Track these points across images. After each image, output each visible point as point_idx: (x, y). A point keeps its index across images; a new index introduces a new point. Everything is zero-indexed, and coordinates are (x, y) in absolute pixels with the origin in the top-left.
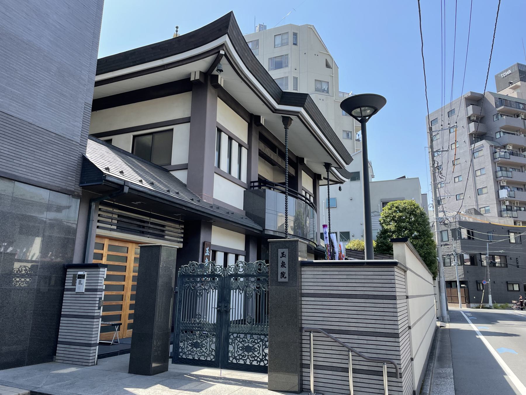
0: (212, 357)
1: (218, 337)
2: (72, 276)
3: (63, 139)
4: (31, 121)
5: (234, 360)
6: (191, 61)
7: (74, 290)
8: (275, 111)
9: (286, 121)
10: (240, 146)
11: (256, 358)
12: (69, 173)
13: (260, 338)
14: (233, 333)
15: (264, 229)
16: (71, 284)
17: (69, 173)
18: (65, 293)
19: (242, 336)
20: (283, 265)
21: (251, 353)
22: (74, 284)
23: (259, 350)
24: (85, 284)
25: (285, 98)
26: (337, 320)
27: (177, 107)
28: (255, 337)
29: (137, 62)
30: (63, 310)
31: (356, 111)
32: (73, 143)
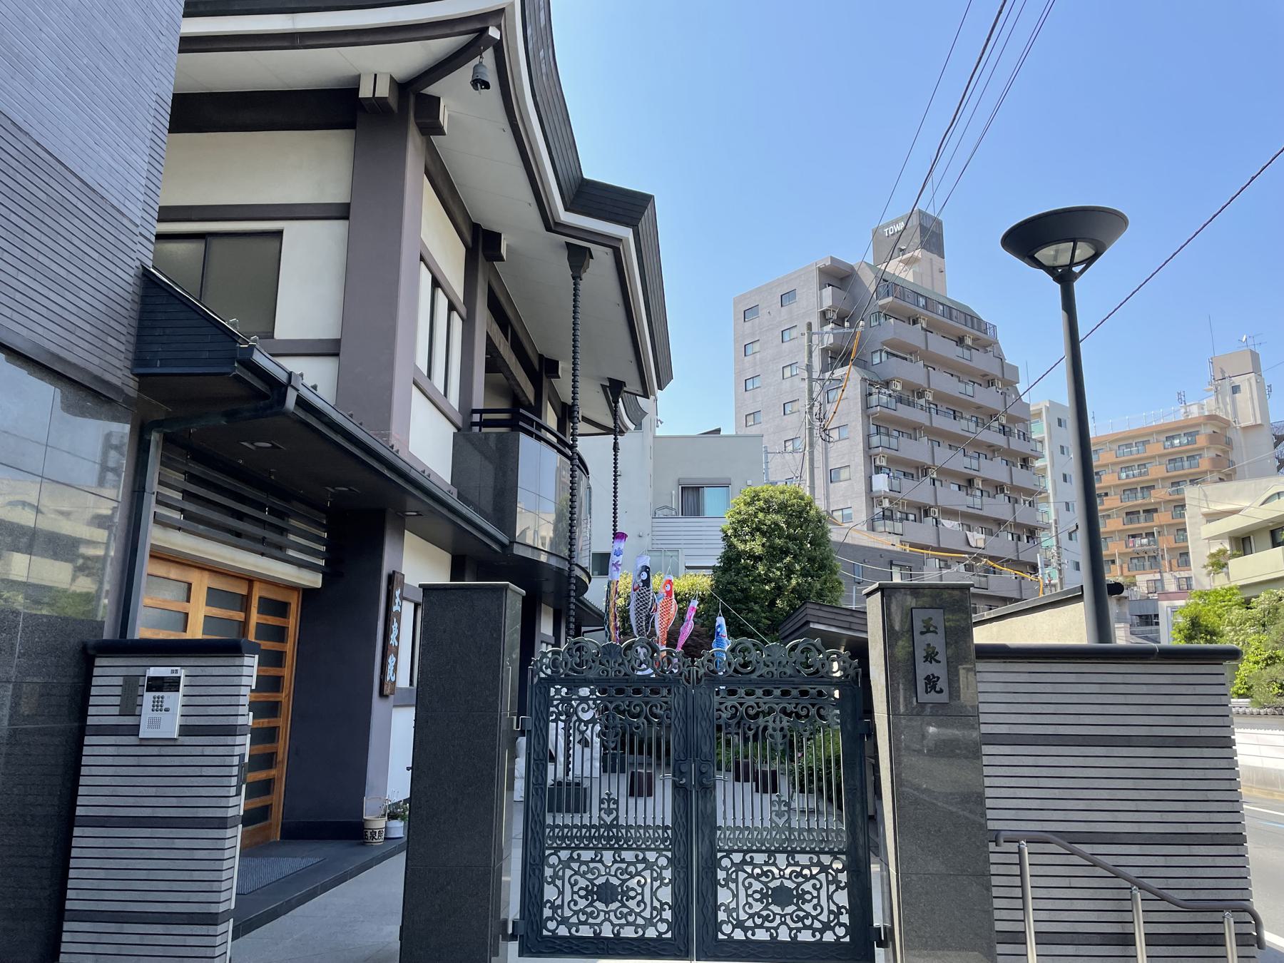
0: (663, 927)
1: (680, 864)
2: (120, 681)
3: (98, 200)
4: (19, 120)
5: (738, 931)
6: (387, 38)
7: (135, 730)
8: (551, 225)
9: (578, 258)
10: (452, 307)
11: (808, 922)
12: (113, 323)
13: (819, 864)
14: (729, 853)
15: (513, 542)
16: (116, 710)
17: (113, 323)
18: (87, 740)
19: (760, 858)
20: (931, 657)
21: (793, 908)
22: (130, 705)
23: (818, 897)
24: (179, 710)
25: (586, 196)
26: (1082, 805)
27: (303, 168)
28: (803, 859)
29: (202, 8)
30: (80, 801)
31: (1045, 254)
32: (125, 222)
